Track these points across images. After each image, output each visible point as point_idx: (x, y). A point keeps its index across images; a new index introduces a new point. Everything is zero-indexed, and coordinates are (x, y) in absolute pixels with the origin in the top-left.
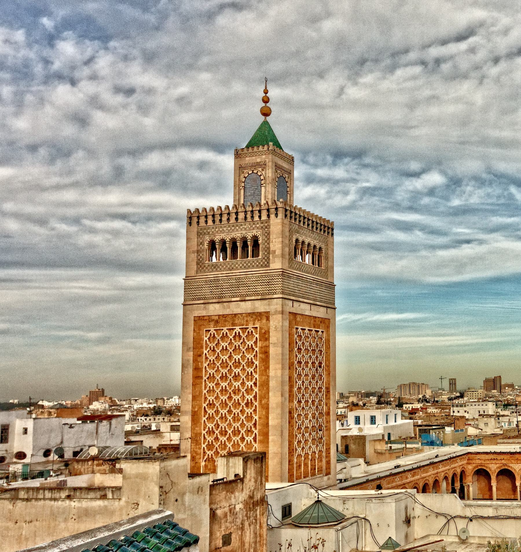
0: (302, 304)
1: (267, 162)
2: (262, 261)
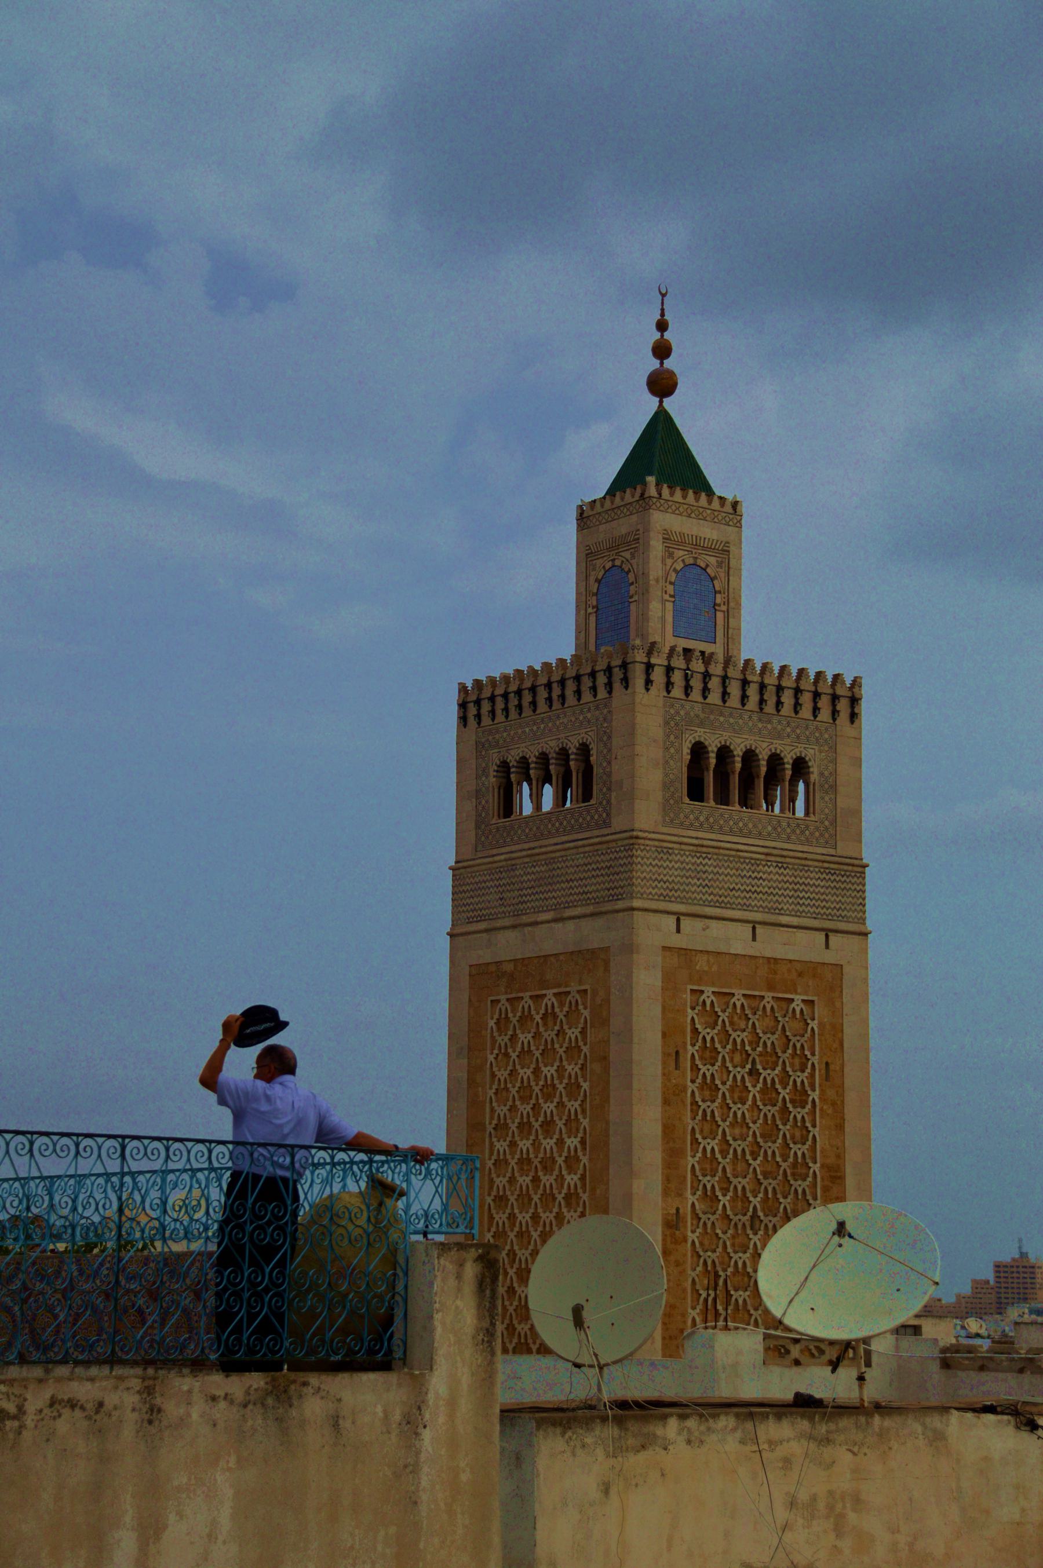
0: (713, 924)
1: (641, 532)
2: (597, 811)
